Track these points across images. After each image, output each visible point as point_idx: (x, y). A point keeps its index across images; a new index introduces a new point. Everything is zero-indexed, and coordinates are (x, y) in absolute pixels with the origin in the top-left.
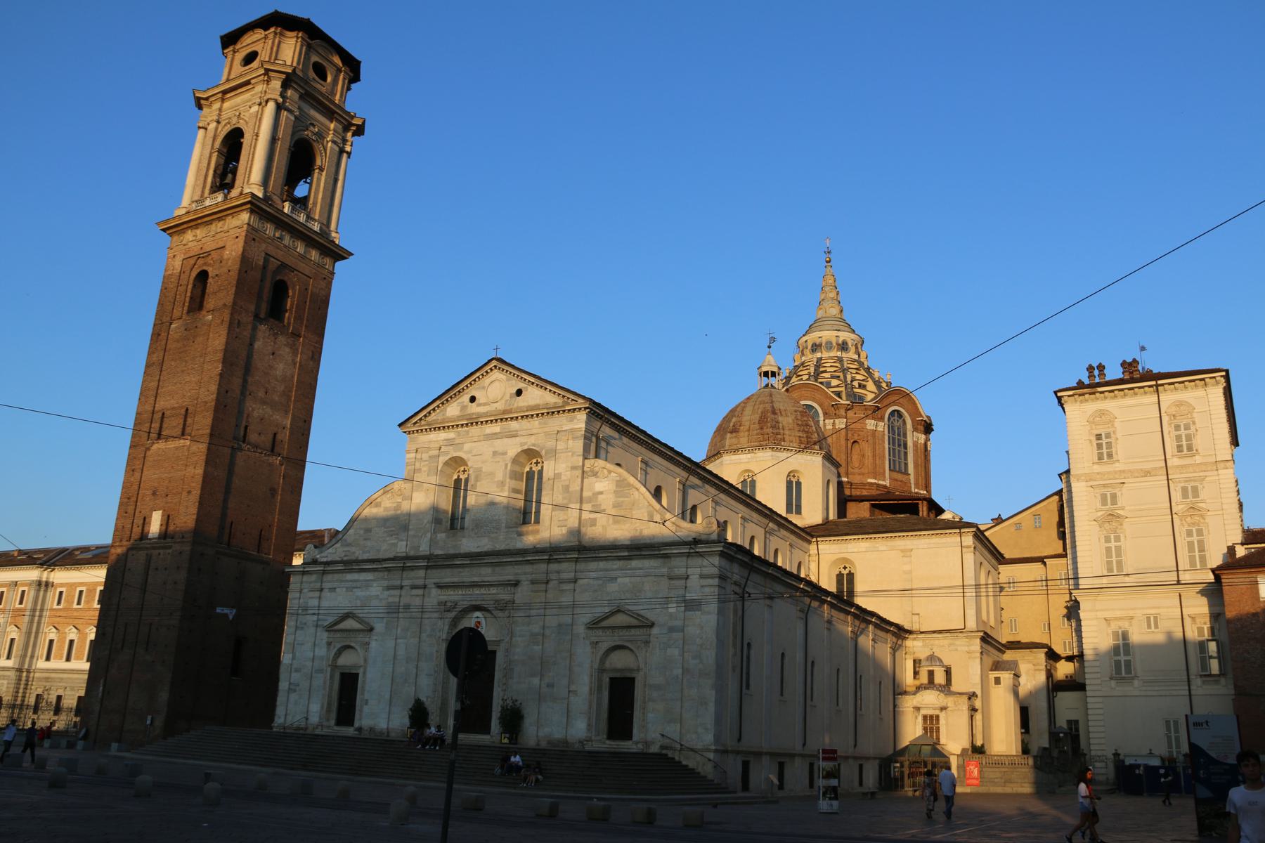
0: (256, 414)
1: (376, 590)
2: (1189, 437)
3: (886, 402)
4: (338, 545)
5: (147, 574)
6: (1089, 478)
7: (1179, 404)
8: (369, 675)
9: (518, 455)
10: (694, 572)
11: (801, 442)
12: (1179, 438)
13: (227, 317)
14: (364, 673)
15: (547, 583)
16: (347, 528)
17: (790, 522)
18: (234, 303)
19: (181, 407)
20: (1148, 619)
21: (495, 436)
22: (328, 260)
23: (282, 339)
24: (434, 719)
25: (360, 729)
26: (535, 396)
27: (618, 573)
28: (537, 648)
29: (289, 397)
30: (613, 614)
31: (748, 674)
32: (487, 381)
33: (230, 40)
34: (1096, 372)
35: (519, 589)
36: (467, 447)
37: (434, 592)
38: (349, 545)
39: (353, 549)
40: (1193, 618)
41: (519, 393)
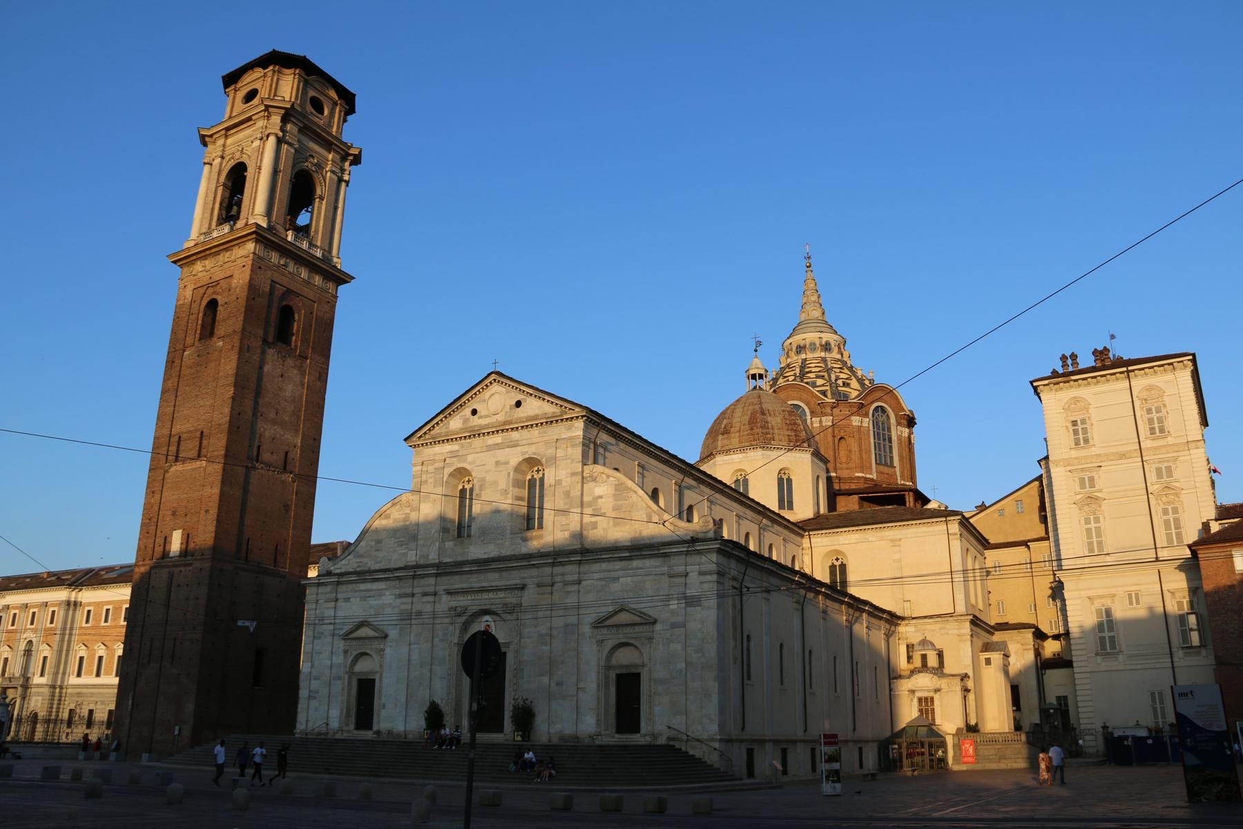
0: (267, 434)
1: (388, 598)
2: (1160, 420)
3: (870, 399)
4: (351, 557)
5: (169, 591)
6: (1067, 463)
7: (1150, 388)
8: (385, 681)
9: (520, 464)
10: (693, 570)
11: (790, 441)
12: (1151, 421)
13: (237, 342)
15: (552, 585)
16: (359, 540)
17: (783, 518)
18: (244, 329)
19: (196, 431)
20: (1130, 595)
21: (497, 446)
22: (331, 285)
23: (290, 362)
24: (449, 720)
25: (378, 733)
26: (534, 407)
27: (620, 573)
28: (546, 648)
29: (299, 417)
30: (616, 613)
31: (749, 666)
32: (487, 394)
33: (231, 80)
34: (1069, 362)
35: (526, 593)
36: (470, 458)
37: (445, 598)
38: (362, 556)
39: (366, 560)
40: (1173, 593)
41: (518, 404)
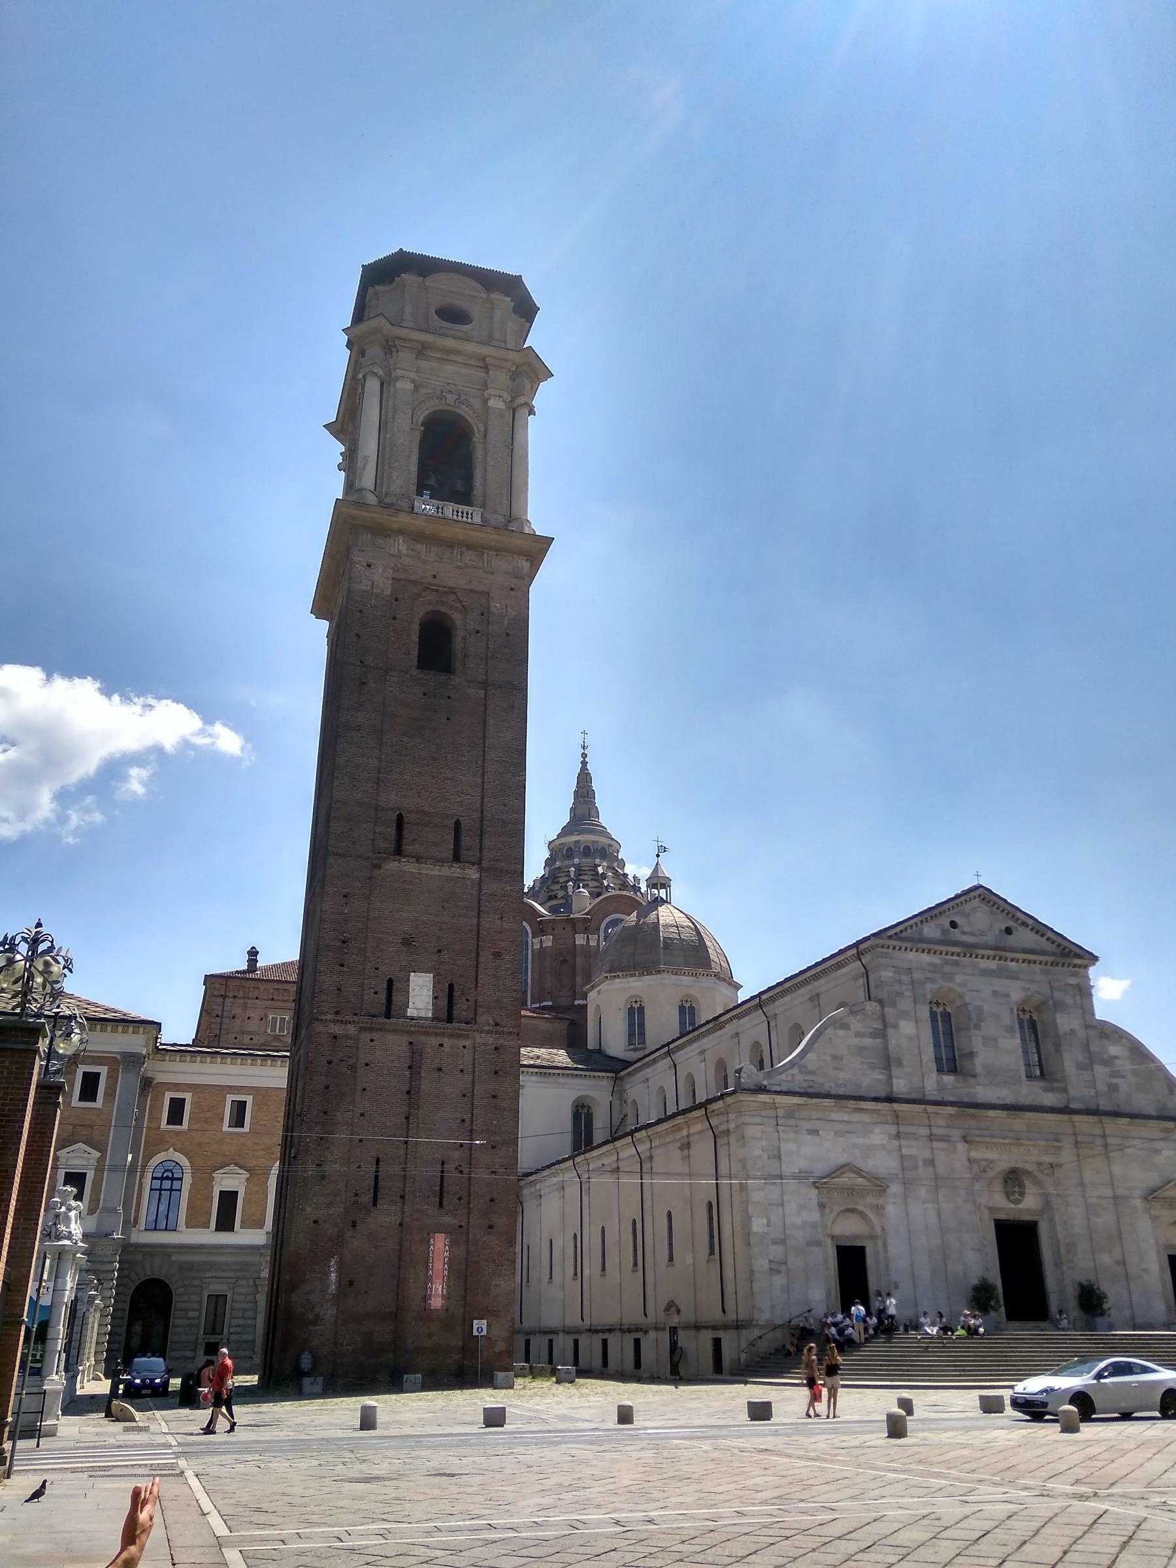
14: (885, 1246)
32: (967, 908)
36: (959, 978)
37: (961, 1147)
39: (820, 1080)
